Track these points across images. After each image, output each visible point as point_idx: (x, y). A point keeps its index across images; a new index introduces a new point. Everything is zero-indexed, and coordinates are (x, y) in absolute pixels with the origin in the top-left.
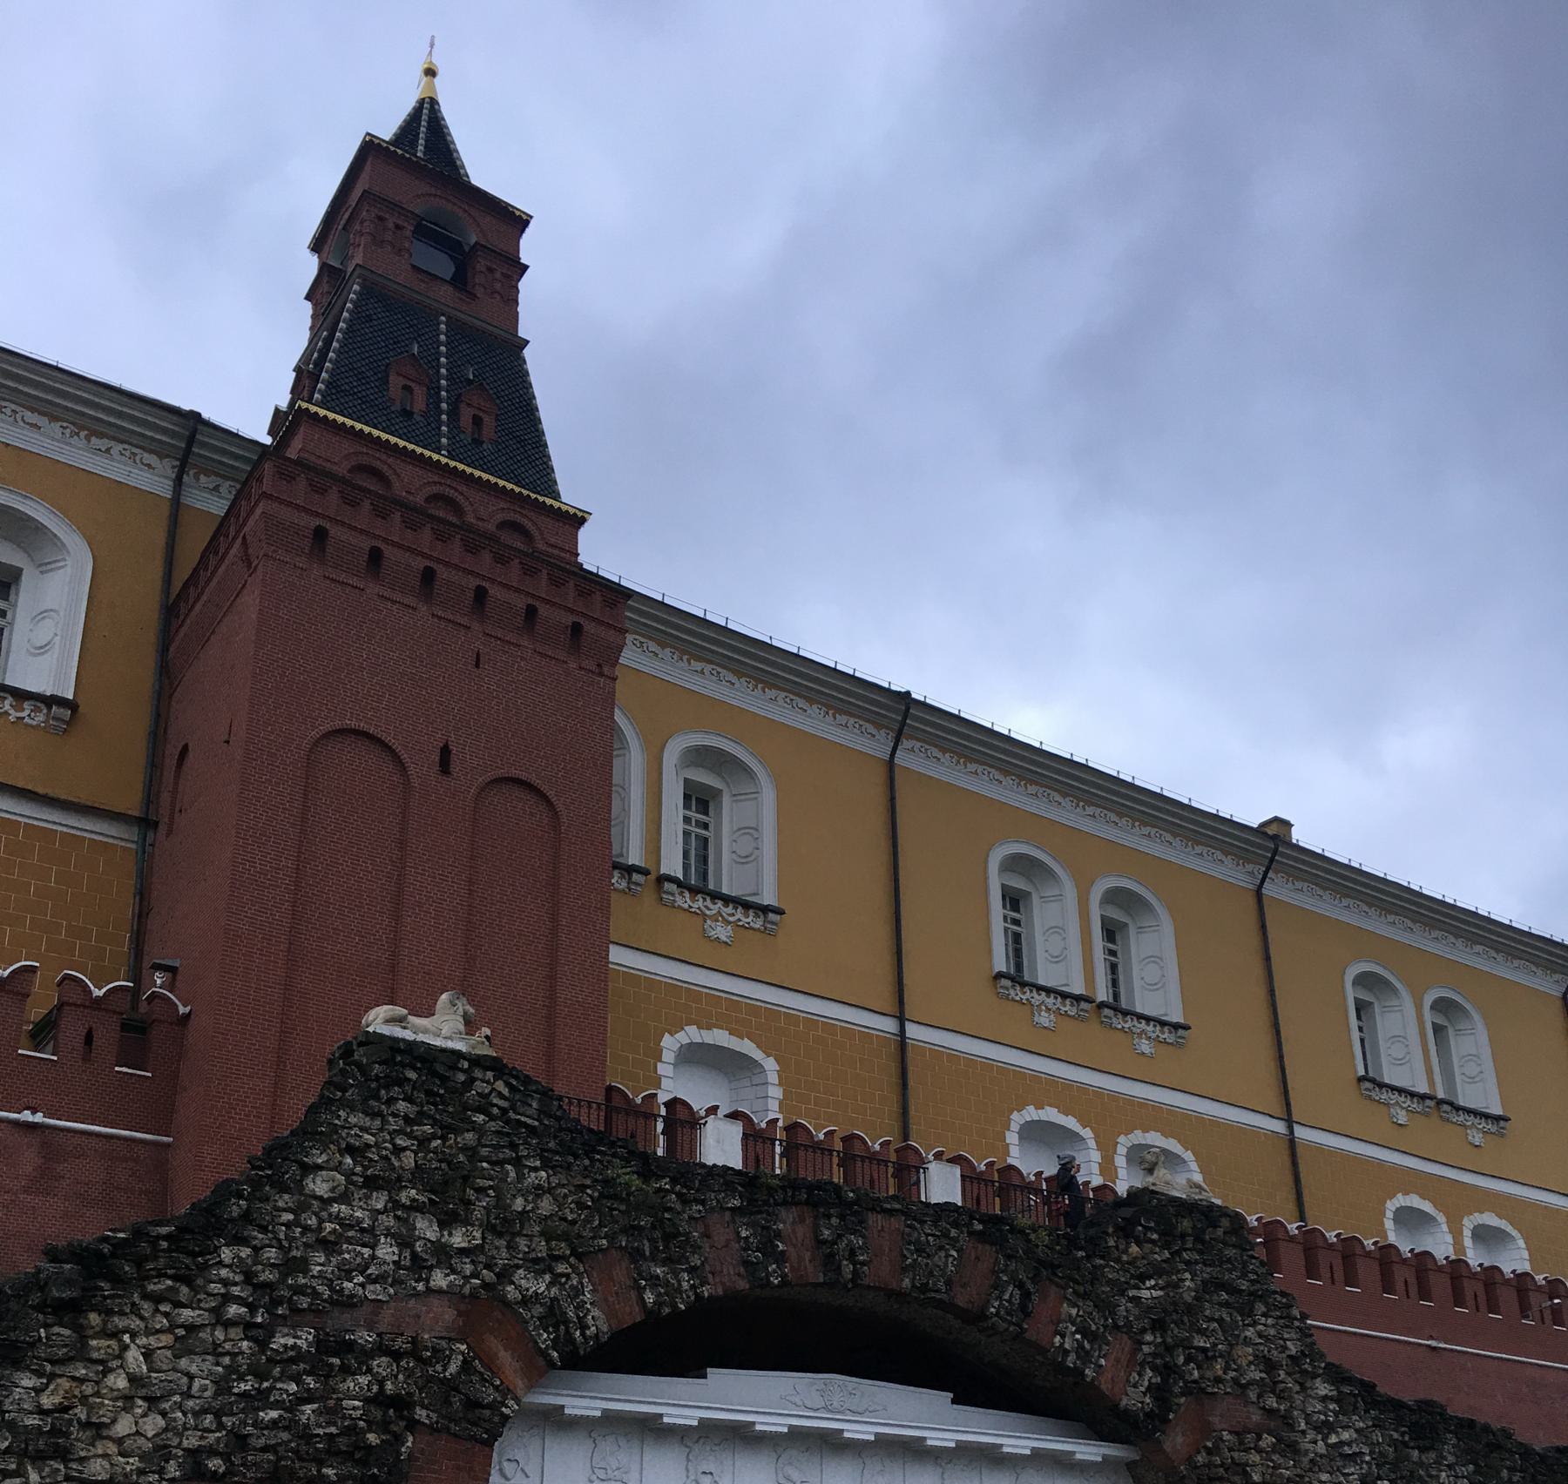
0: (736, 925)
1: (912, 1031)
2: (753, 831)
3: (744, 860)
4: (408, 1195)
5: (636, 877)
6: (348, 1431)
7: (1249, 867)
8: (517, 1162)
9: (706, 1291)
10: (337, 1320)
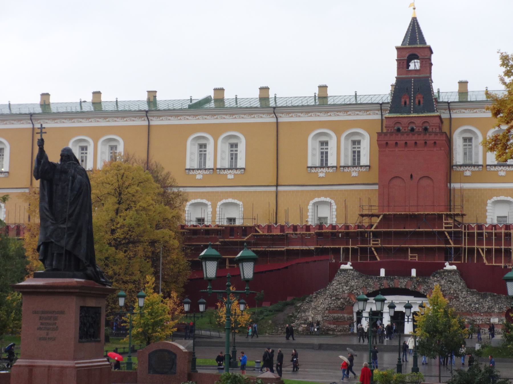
0: (506, 171)
4: (343, 285)
5: (481, 167)
8: (354, 280)
10: (337, 296)
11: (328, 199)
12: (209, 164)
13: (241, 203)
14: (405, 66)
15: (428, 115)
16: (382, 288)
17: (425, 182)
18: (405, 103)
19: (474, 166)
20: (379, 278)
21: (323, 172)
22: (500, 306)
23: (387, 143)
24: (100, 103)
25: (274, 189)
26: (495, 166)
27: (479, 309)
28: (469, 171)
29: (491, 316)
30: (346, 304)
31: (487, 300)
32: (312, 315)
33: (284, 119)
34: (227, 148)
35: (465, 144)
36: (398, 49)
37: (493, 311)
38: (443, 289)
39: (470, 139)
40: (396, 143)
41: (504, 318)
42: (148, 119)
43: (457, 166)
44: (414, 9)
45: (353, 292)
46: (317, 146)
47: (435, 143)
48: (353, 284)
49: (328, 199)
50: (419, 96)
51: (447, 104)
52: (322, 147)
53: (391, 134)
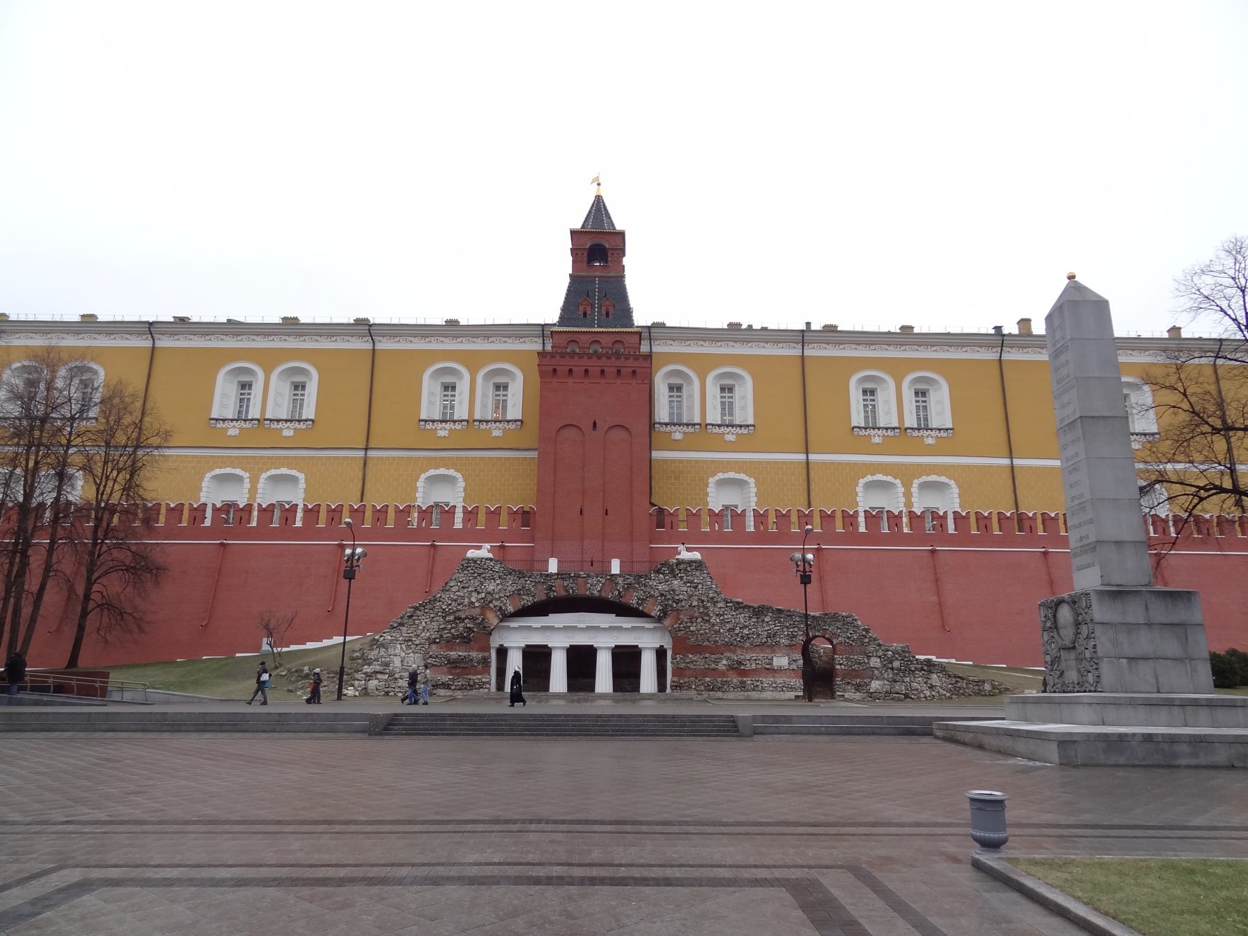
0: (737, 434)
1: (812, 457)
2: (744, 398)
3: (743, 408)
6: (460, 633)
7: (994, 350)
8: (494, 579)
9: (536, 600)
11: (451, 472)
12: (254, 412)
13: (301, 476)
16: (552, 595)
17: (616, 435)
18: (585, 314)
19: (688, 425)
20: (547, 575)
21: (446, 429)
22: (791, 632)
23: (555, 370)
25: (362, 453)
26: (719, 426)
27: (749, 638)
28: (679, 432)
29: (773, 652)
30: (475, 630)
31: (766, 620)
32: (403, 654)
33: (384, 345)
34: (287, 389)
35: (671, 394)
36: (574, 233)
37: (778, 643)
38: (677, 598)
39: (679, 388)
40: (571, 371)
41: (799, 656)
42: (152, 337)
43: (660, 424)
44: (599, 184)
45: (491, 605)
46: (438, 389)
47: (634, 372)
48: (493, 588)
49: (451, 472)
50: (607, 303)
52: (446, 393)
53: (563, 356)
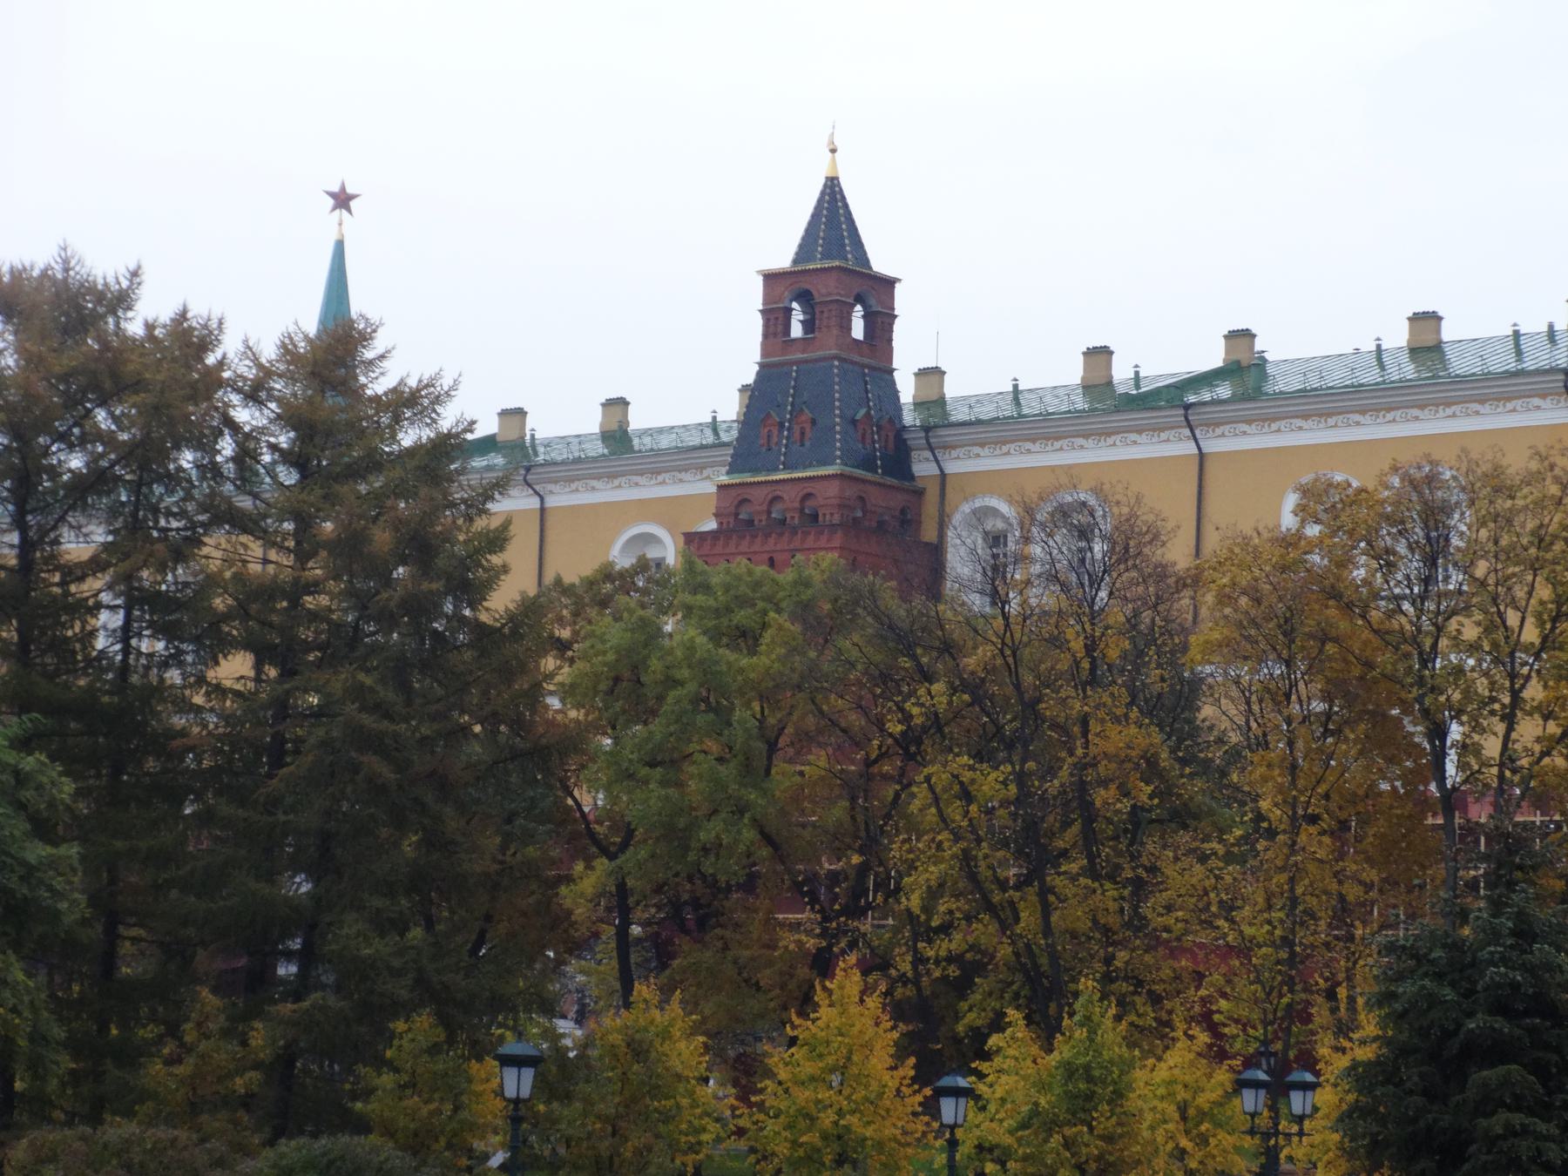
14: (780, 328)
15: (815, 474)
24: (941, 401)
33: (559, 499)
44: (833, 151)
51: (1182, 412)
